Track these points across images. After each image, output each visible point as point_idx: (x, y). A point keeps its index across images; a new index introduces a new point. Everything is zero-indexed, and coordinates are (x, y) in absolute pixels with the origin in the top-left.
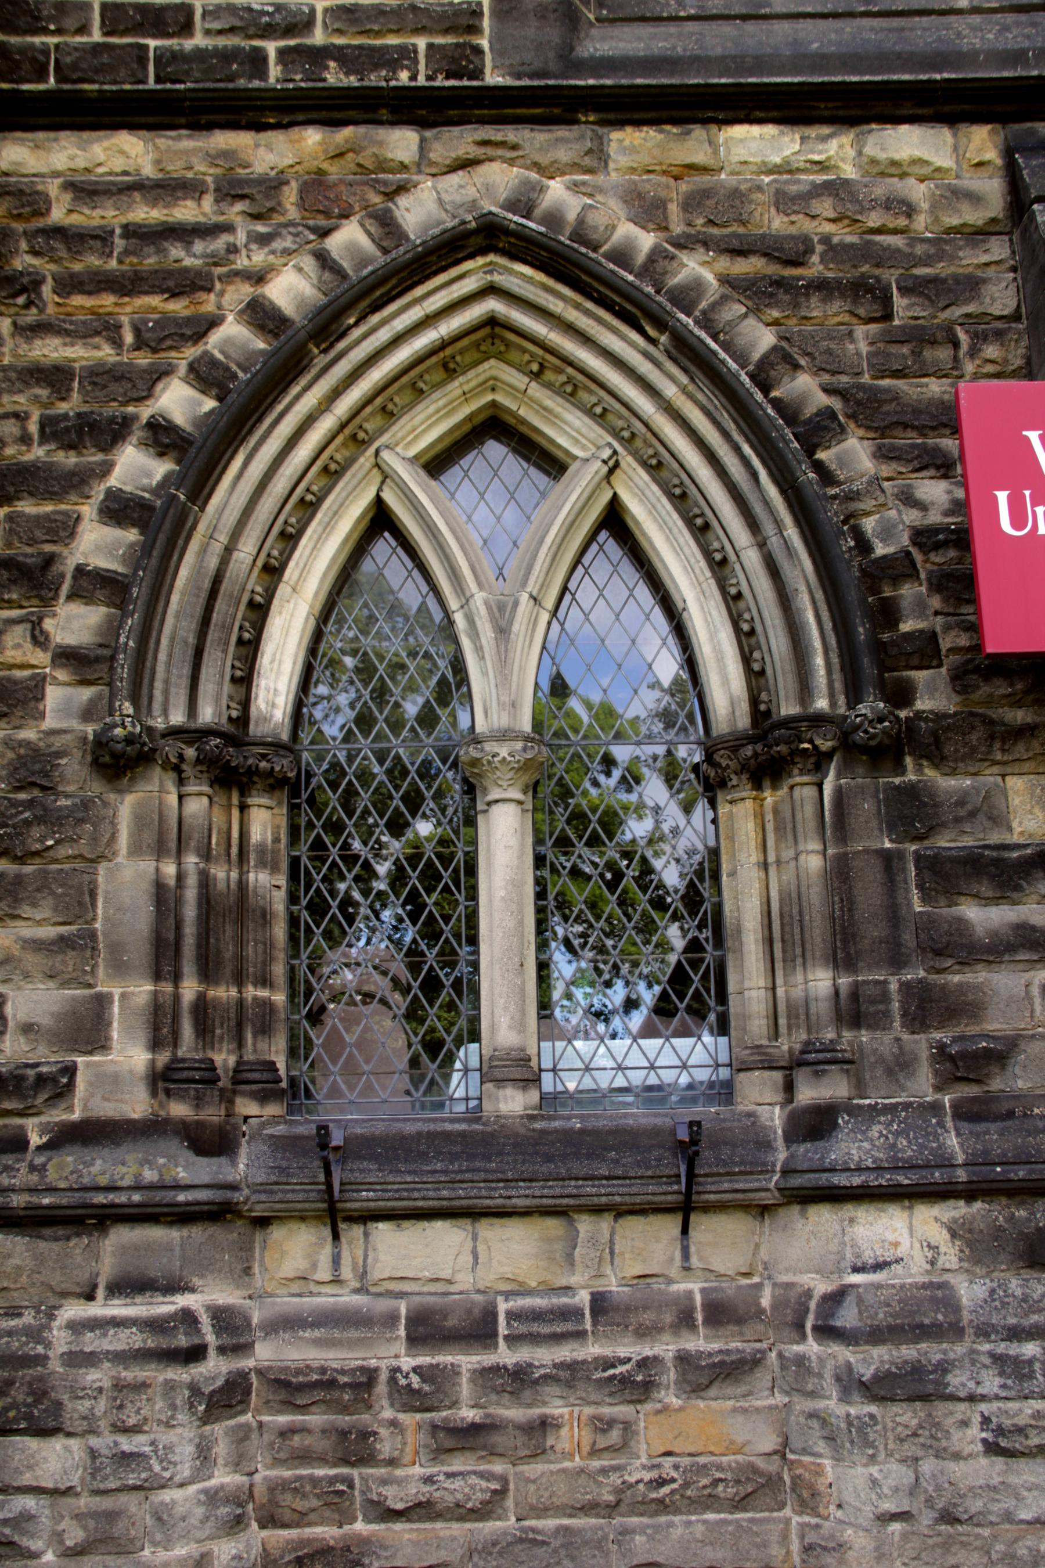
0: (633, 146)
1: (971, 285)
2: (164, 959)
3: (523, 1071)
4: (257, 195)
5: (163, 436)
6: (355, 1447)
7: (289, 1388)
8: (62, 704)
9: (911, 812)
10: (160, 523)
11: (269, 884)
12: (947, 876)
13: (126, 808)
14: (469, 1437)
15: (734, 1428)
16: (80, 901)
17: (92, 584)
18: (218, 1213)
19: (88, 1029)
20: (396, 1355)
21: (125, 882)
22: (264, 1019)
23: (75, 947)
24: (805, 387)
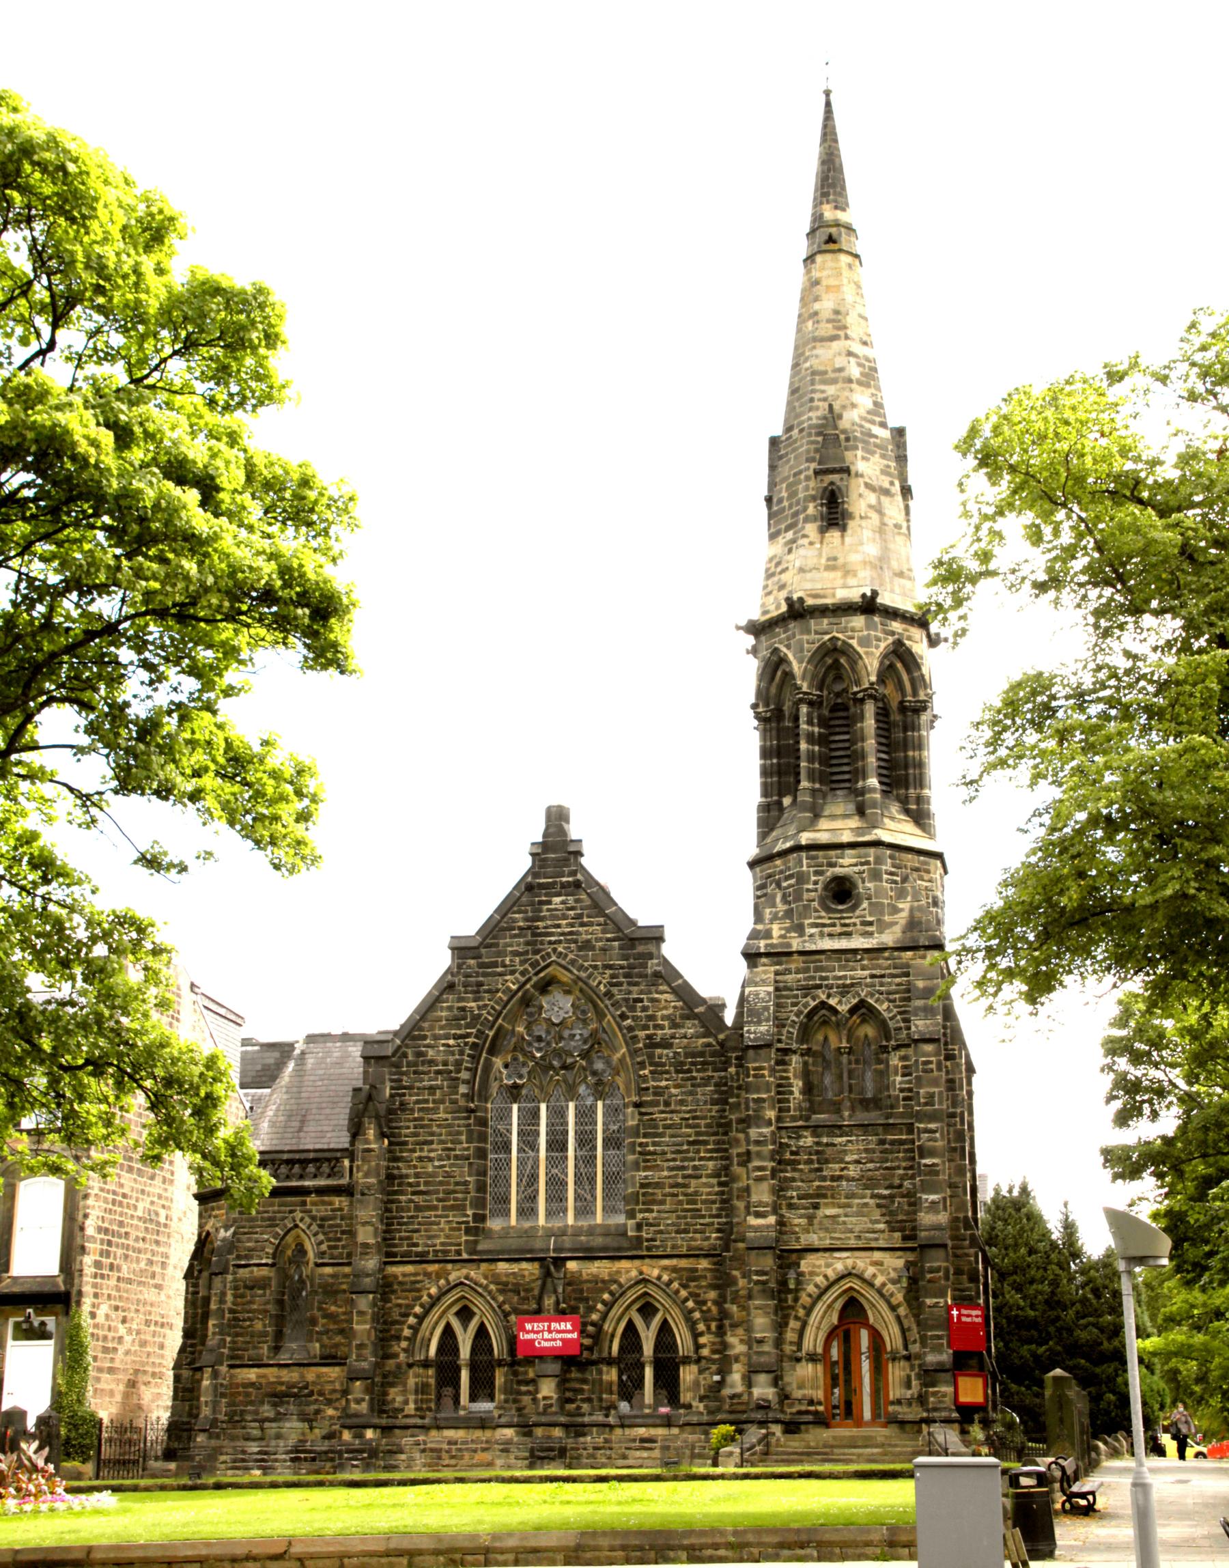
0: (484, 1266)
2: (416, 1392)
3: (465, 1408)
4: (428, 1275)
5: (416, 1316)
6: (440, 1458)
7: (432, 1450)
8: (402, 1356)
9: (515, 1374)
10: (415, 1329)
11: (432, 1381)
12: (519, 1383)
13: (411, 1372)
14: (453, 1457)
15: (487, 1456)
16: (405, 1385)
17: (407, 1339)
18: (422, 1427)
19: (406, 1402)
20: (446, 1447)
21: (412, 1382)
23: (404, 1392)
24: (507, 1307)
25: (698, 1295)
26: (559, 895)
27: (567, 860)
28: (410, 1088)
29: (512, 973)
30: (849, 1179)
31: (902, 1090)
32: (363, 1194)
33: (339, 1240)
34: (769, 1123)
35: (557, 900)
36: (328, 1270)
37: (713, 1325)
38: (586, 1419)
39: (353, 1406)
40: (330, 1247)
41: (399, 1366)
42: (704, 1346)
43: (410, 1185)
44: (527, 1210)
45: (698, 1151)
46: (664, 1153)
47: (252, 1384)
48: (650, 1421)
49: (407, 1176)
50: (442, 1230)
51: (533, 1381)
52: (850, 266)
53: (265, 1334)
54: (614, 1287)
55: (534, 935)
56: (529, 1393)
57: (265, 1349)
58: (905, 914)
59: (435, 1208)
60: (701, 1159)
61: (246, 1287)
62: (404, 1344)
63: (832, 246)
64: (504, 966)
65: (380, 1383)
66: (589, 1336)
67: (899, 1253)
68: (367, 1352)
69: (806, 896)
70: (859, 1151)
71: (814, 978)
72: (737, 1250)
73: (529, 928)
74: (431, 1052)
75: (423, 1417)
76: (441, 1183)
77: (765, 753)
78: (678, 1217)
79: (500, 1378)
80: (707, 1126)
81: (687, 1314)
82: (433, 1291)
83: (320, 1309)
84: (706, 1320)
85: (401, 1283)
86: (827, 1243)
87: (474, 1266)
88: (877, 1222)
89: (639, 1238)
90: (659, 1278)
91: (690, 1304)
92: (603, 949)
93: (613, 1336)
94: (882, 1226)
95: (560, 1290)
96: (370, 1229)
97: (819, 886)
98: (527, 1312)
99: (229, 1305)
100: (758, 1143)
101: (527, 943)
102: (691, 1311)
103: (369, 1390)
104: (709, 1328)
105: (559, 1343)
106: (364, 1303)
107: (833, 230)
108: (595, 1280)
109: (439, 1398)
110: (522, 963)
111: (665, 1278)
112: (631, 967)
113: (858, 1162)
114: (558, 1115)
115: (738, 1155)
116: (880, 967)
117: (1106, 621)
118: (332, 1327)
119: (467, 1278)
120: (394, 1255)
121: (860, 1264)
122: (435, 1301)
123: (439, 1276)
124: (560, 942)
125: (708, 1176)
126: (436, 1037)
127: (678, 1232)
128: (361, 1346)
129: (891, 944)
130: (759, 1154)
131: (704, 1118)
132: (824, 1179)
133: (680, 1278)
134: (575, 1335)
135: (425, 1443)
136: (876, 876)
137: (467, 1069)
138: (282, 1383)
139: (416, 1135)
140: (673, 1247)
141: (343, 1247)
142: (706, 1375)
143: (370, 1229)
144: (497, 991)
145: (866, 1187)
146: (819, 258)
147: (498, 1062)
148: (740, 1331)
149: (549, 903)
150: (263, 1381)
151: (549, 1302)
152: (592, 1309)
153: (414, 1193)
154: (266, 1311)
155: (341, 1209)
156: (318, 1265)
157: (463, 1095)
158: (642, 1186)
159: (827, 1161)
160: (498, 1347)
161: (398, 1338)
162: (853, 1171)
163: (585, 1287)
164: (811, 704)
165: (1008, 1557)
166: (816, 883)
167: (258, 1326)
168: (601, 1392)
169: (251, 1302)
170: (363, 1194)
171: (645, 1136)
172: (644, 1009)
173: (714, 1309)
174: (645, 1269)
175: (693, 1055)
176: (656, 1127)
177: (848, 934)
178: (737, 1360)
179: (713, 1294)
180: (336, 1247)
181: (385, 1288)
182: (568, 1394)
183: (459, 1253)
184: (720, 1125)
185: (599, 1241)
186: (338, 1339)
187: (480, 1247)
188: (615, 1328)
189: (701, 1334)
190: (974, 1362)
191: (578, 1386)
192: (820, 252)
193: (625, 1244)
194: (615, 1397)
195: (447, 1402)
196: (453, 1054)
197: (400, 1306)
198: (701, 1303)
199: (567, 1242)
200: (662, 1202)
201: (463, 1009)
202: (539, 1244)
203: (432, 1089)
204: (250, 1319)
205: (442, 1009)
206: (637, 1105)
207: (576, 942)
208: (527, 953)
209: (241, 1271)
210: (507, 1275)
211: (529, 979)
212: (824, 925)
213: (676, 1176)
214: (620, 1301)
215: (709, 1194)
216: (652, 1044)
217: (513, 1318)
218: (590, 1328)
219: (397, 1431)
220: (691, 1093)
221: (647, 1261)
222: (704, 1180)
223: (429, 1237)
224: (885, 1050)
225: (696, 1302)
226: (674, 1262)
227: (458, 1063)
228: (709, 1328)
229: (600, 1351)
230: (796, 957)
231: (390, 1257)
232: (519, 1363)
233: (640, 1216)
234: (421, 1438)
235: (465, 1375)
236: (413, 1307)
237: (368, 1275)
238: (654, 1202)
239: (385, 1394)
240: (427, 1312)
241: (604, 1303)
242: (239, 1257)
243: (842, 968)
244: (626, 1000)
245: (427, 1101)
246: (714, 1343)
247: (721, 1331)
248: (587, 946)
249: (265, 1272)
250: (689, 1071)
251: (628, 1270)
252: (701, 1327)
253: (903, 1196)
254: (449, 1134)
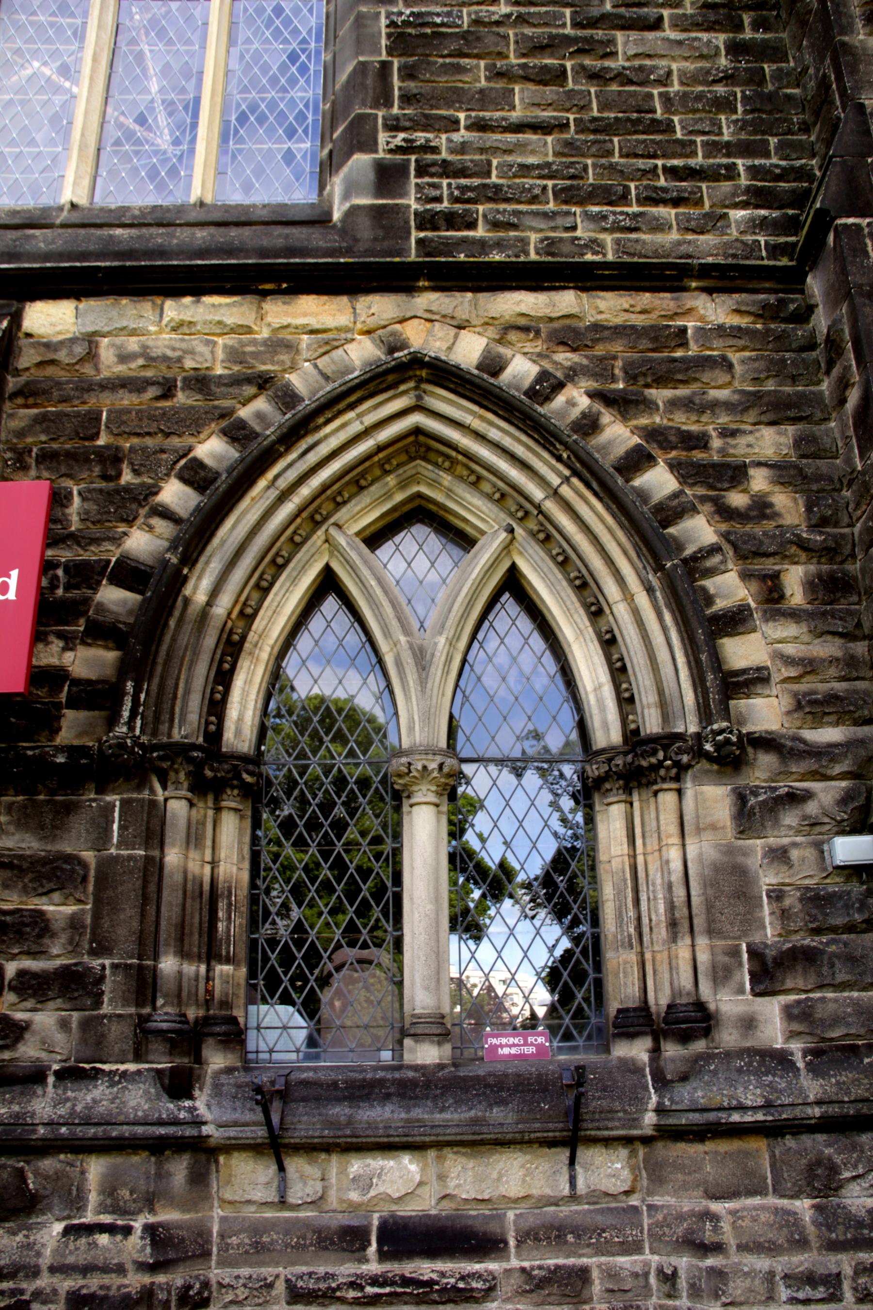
25: (700, 441)
37: (795, 579)
38: (44, 1106)
42: (752, 681)
48: (452, 1116)
54: (256, 409)
66: (102, 631)
78: (570, 148)
84: (753, 544)
93: (232, 648)
102: (671, 512)
104: (772, 594)
127: (566, 196)
133: (601, 369)
163: (106, 404)
168: (148, 944)
173: (789, 507)
189: (735, 621)
194: (229, 974)
214: (286, 468)
218: (113, 597)
221: (428, 300)
226: (566, 301)
229: (161, 710)
241: (196, 475)
246: (810, 666)
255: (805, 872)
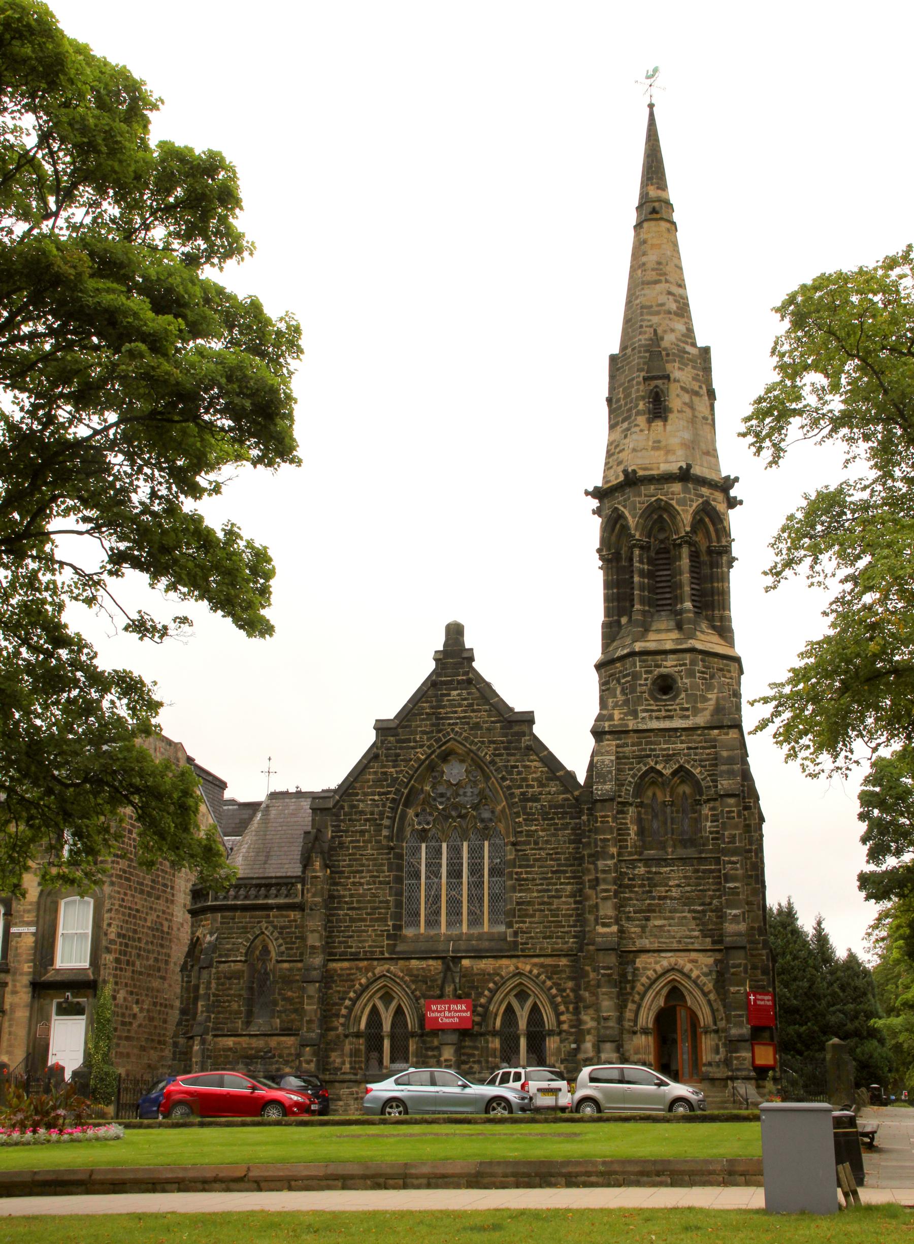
0: (401, 963)
1: (436, 980)
2: (351, 1056)
3: (387, 1068)
4: (359, 969)
5: (350, 999)
8: (340, 1029)
9: (424, 1042)
10: (350, 1009)
11: (363, 1047)
12: (427, 1049)
13: (347, 1041)
16: (342, 1050)
17: (343, 1016)
19: (343, 1063)
21: (347, 1048)
22: (361, 1062)
23: (342, 1056)
24: (418, 993)
26: (456, 689)
27: (462, 663)
28: (346, 831)
29: (422, 746)
30: (672, 899)
31: (711, 833)
32: (311, 910)
33: (294, 943)
34: (612, 857)
35: (455, 693)
36: (286, 965)
37: (571, 1007)
39: (304, 1065)
40: (287, 949)
41: (338, 1036)
42: (564, 1022)
43: (346, 903)
44: (433, 922)
45: (559, 878)
46: (534, 879)
47: (230, 1049)
49: (344, 896)
50: (370, 936)
51: (438, 1048)
52: (668, 230)
53: (238, 1012)
54: (497, 978)
55: (437, 718)
56: (434, 1056)
57: (239, 1024)
58: (712, 702)
59: (364, 920)
60: (561, 884)
61: (225, 977)
62: (342, 1020)
63: (655, 216)
64: (416, 741)
65: (323, 1049)
66: (479, 1015)
67: (710, 954)
68: (315, 1026)
69: (639, 689)
70: (680, 878)
71: (645, 750)
72: (588, 951)
73: (434, 714)
74: (361, 805)
75: (356, 1074)
76: (369, 902)
77: (608, 585)
78: (545, 927)
79: (412, 1046)
80: (566, 859)
81: (552, 999)
82: (363, 981)
83: (280, 994)
84: (566, 1003)
85: (339, 975)
86: (656, 946)
87: (394, 962)
88: (693, 930)
89: (515, 943)
90: (531, 972)
91: (554, 991)
92: (488, 729)
93: (496, 1015)
94: (696, 933)
95: (457, 980)
96: (316, 935)
97: (649, 682)
98: (432, 997)
99: (213, 990)
100: (604, 871)
101: (432, 725)
102: (555, 996)
103: (315, 1054)
104: (567, 1009)
105: (457, 1020)
106: (312, 989)
107: (656, 204)
108: (483, 973)
109: (368, 1060)
110: (429, 739)
111: (535, 972)
112: (509, 742)
113: (678, 886)
114: (455, 852)
115: (589, 881)
116: (695, 742)
117: (885, 457)
118: (289, 1007)
119: (388, 971)
120: (335, 954)
121: (681, 962)
122: (365, 988)
123: (367, 970)
124: (456, 724)
125: (567, 896)
126: (365, 794)
127: (544, 938)
128: (310, 1022)
129: (702, 725)
130: (604, 880)
131: (564, 853)
132: (653, 898)
133: (547, 972)
134: (468, 1014)
135: (357, 1093)
136: (691, 674)
137: (388, 817)
138: (252, 1049)
139: (350, 866)
140: (541, 949)
141: (297, 948)
142: (566, 1044)
143: (316, 935)
144: (411, 760)
145: (685, 905)
146: (645, 225)
147: (411, 812)
148: (591, 1011)
149: (449, 695)
150: (238, 1047)
151: (449, 989)
152: (481, 995)
153: (349, 909)
154: (240, 995)
155: (295, 921)
156: (278, 962)
157: (385, 837)
158: (518, 904)
159: (655, 886)
160: (411, 1022)
161: (337, 1016)
162: (675, 893)
164: (642, 548)
165: (839, 1185)
166: (646, 679)
167: (235, 1006)
169: (230, 989)
170: (311, 910)
171: (520, 867)
172: (519, 773)
174: (520, 965)
175: (556, 807)
176: (528, 860)
177: (670, 717)
178: (589, 1032)
179: (570, 984)
180: (291, 949)
181: (327, 979)
182: (463, 1058)
183: (382, 953)
184: (575, 859)
185: (486, 945)
186: (293, 1016)
187: (398, 949)
188: (498, 1009)
189: (562, 1013)
190: (767, 1034)
191: (471, 1052)
192: (646, 220)
193: (506, 947)
194: (498, 1060)
195: (374, 1063)
196: (377, 806)
197: (339, 992)
198: (561, 990)
199: (463, 945)
200: (533, 916)
201: (385, 773)
202: (441, 947)
203: (362, 832)
204: (229, 1001)
205: (370, 773)
206: (514, 844)
207: (468, 723)
208: (432, 732)
209: (222, 965)
210: (418, 969)
211: (434, 752)
212: (652, 711)
213: (543, 897)
214: (501, 989)
215: (567, 910)
216: (525, 798)
217: (422, 1001)
218: (479, 1009)
219: (337, 1084)
220: (554, 835)
221: (522, 959)
222: (564, 899)
223: (360, 942)
224: (698, 803)
225: (558, 990)
226: (541, 960)
227: (382, 814)
228: (567, 1009)
229: (487, 1026)
230: (631, 734)
231: (331, 955)
232: (427, 1035)
233: (516, 926)
234: (354, 1090)
235: (387, 1043)
236: (348, 993)
237: (315, 969)
238: (527, 916)
239: (328, 1057)
240: (359, 996)
241: (490, 990)
242: (220, 956)
243: (666, 742)
244: (506, 767)
245: (358, 841)
246: (571, 1020)
247: (577, 1011)
248: (477, 726)
249: (239, 966)
250: (553, 819)
251: (507, 966)
252: (562, 1008)
253: (712, 911)
254: (374, 865)
255: (568, 1049)
